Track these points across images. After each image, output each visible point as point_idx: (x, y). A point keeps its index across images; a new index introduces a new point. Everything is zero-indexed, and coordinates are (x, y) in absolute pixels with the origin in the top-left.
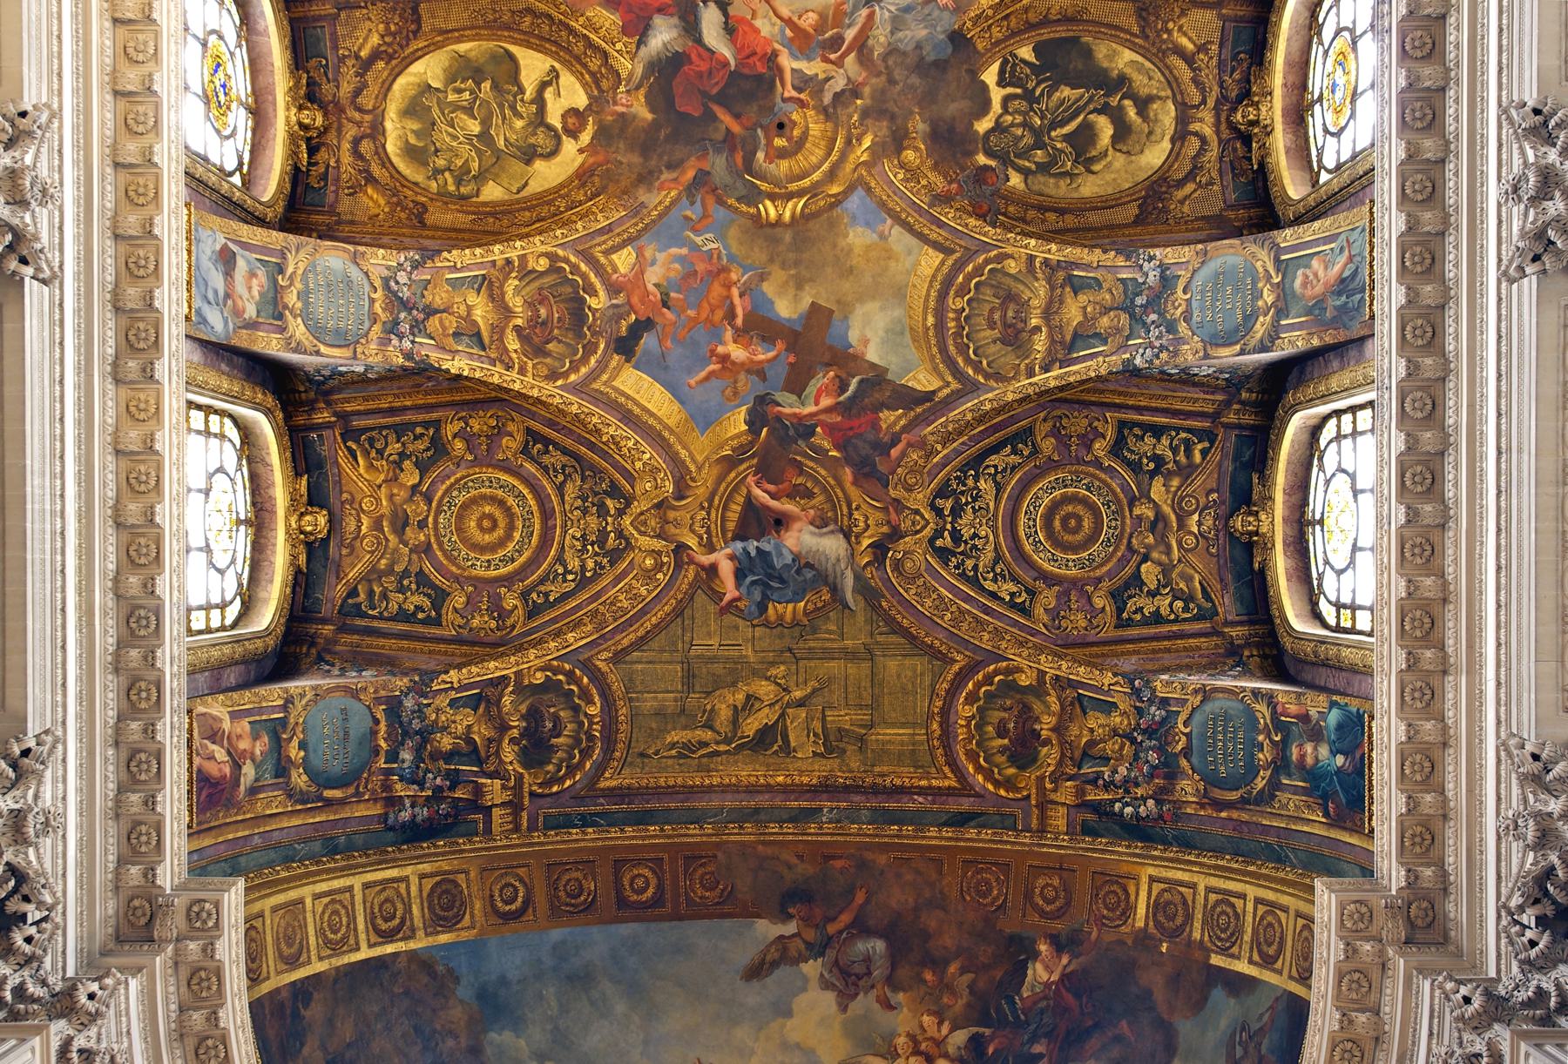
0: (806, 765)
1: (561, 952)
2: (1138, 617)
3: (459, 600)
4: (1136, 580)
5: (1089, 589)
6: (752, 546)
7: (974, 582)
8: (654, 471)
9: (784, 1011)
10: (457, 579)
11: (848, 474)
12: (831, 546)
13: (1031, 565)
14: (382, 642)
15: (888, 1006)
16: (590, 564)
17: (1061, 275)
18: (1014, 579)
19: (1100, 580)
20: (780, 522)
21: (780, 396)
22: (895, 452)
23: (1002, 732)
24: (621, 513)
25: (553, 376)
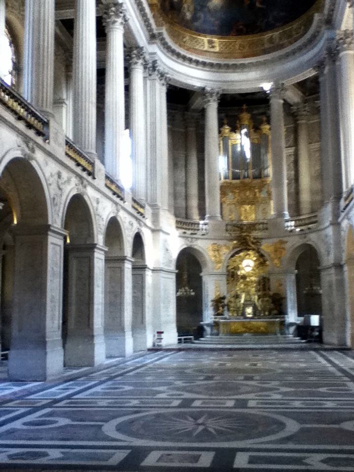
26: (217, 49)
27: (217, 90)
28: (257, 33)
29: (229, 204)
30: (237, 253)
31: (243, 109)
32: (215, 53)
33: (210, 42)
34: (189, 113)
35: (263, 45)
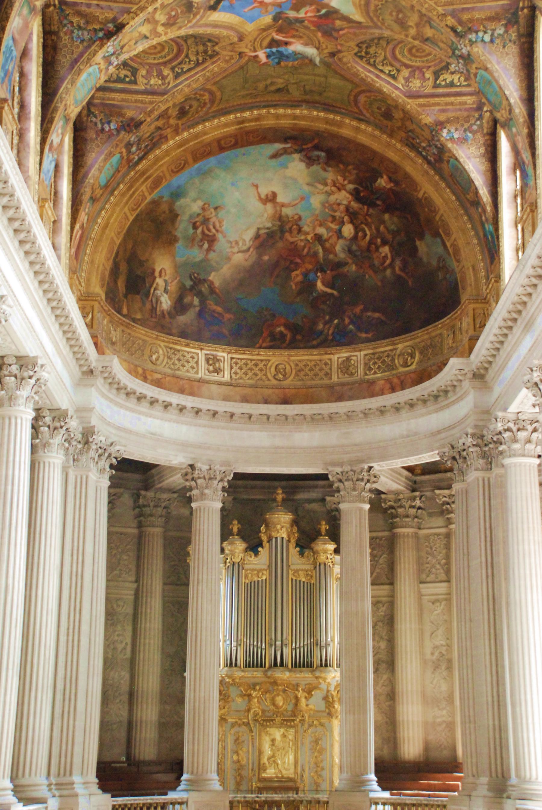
0: (296, 93)
1: (199, 169)
2: (443, 83)
3: (143, 72)
4: (446, 67)
5: (424, 70)
6: (274, 50)
7: (374, 65)
8: (228, 37)
9: (284, 166)
10: (141, 64)
11: (319, 34)
12: (311, 51)
13: (399, 61)
15: (325, 170)
16: (201, 59)
17: (425, 19)
18: (392, 65)
19: (430, 67)
20: (286, 44)
21: (287, 12)
22: (341, 32)
23: (379, 108)
24: (214, 46)
25: (180, 28)
26: (227, 377)
28: (314, 347)
32: (220, 384)
33: (212, 360)
35: (328, 375)
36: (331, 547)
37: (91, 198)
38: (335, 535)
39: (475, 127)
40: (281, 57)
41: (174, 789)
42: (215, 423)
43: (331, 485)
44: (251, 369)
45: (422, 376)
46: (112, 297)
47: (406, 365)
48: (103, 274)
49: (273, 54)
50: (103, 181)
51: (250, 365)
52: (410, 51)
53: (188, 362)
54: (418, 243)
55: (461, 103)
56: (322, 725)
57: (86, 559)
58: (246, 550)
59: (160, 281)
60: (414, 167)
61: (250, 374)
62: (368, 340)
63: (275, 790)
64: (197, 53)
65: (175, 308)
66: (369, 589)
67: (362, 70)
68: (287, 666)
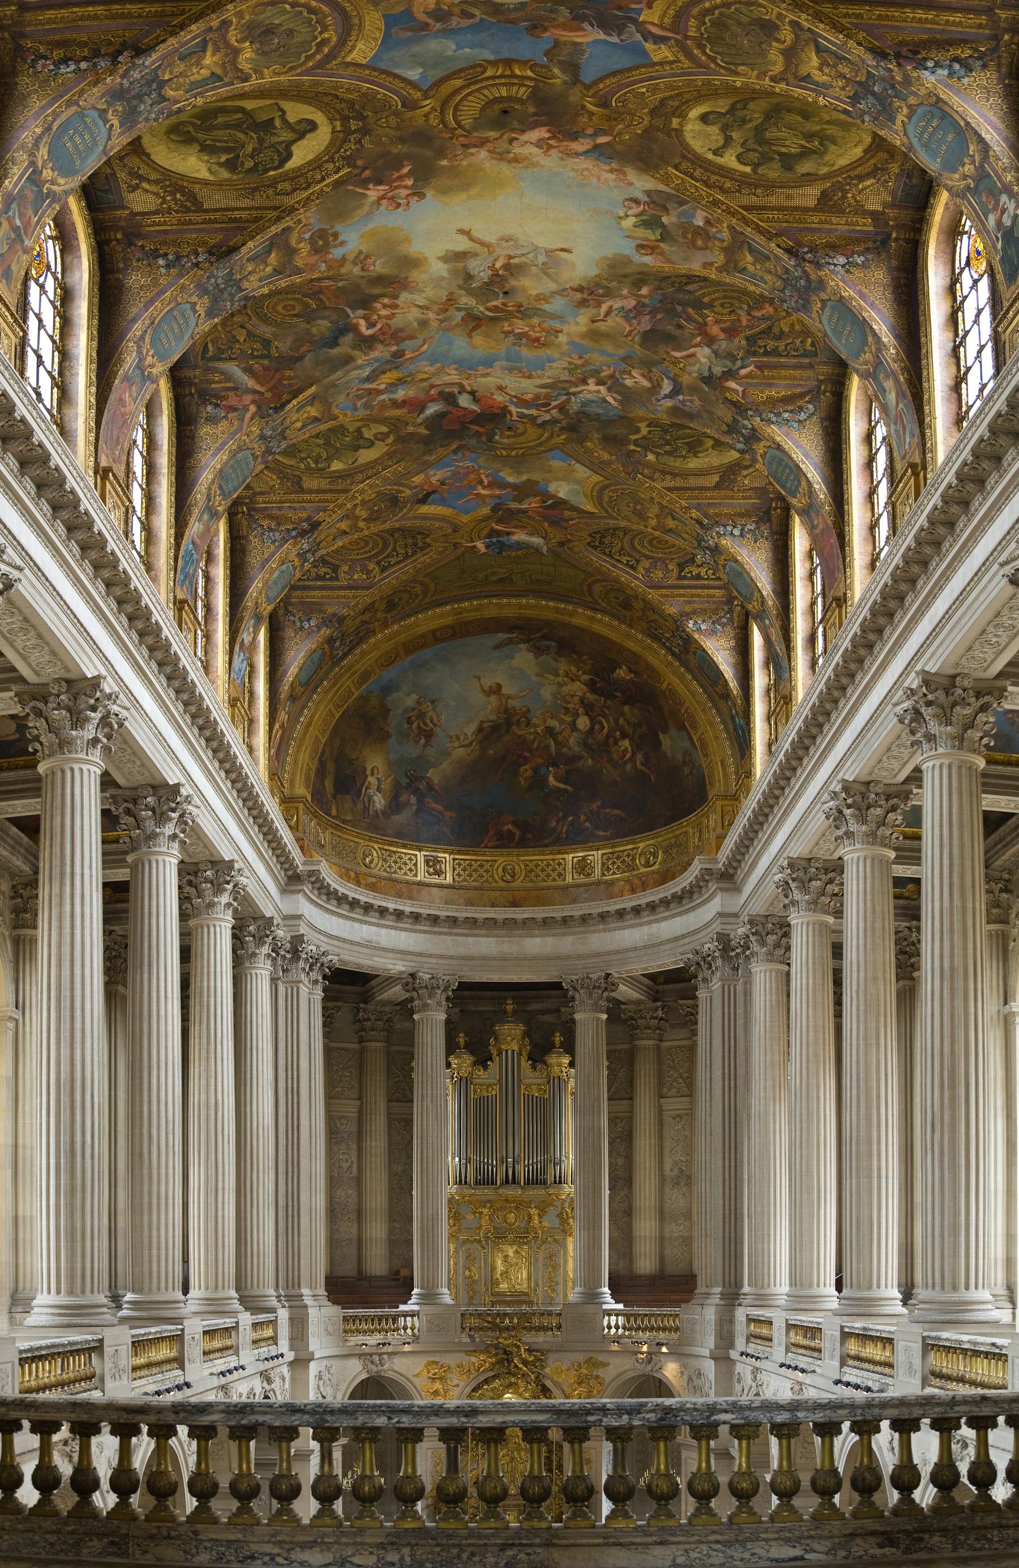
6: (494, 540)
7: (610, 555)
8: (440, 528)
12: (536, 540)
13: (639, 552)
14: (312, 593)
20: (508, 534)
26: (449, 879)
27: (447, 978)
29: (465, 1242)
30: (486, 1381)
31: (505, 1012)
32: (442, 886)
33: (432, 863)
34: (371, 1006)
36: (566, 1060)
37: (291, 696)
38: (569, 1048)
39: (724, 620)
40: (502, 547)
41: (405, 1303)
42: (436, 929)
43: (565, 996)
44: (476, 871)
45: (666, 876)
46: (318, 794)
47: (648, 865)
48: (308, 774)
49: (494, 544)
50: (304, 679)
51: (475, 865)
52: (651, 542)
53: (405, 864)
54: (661, 736)
55: (708, 596)
56: (556, 1241)
57: (301, 1074)
58: (474, 1064)
59: (371, 779)
60: (658, 657)
61: (475, 876)
62: (606, 839)
63: (508, 1304)
64: (406, 545)
65: (390, 807)
66: (605, 1104)
67: (596, 559)
68: (519, 1183)
